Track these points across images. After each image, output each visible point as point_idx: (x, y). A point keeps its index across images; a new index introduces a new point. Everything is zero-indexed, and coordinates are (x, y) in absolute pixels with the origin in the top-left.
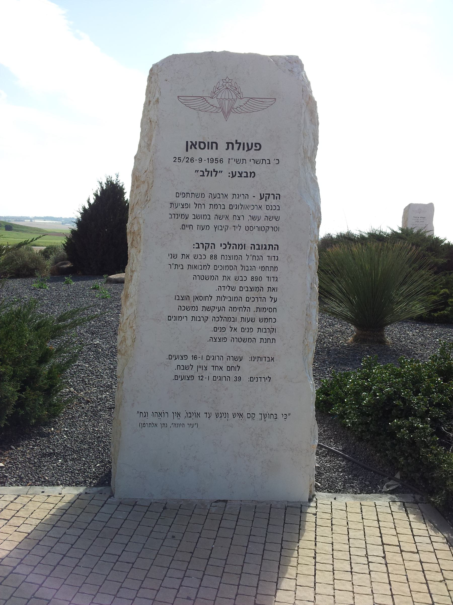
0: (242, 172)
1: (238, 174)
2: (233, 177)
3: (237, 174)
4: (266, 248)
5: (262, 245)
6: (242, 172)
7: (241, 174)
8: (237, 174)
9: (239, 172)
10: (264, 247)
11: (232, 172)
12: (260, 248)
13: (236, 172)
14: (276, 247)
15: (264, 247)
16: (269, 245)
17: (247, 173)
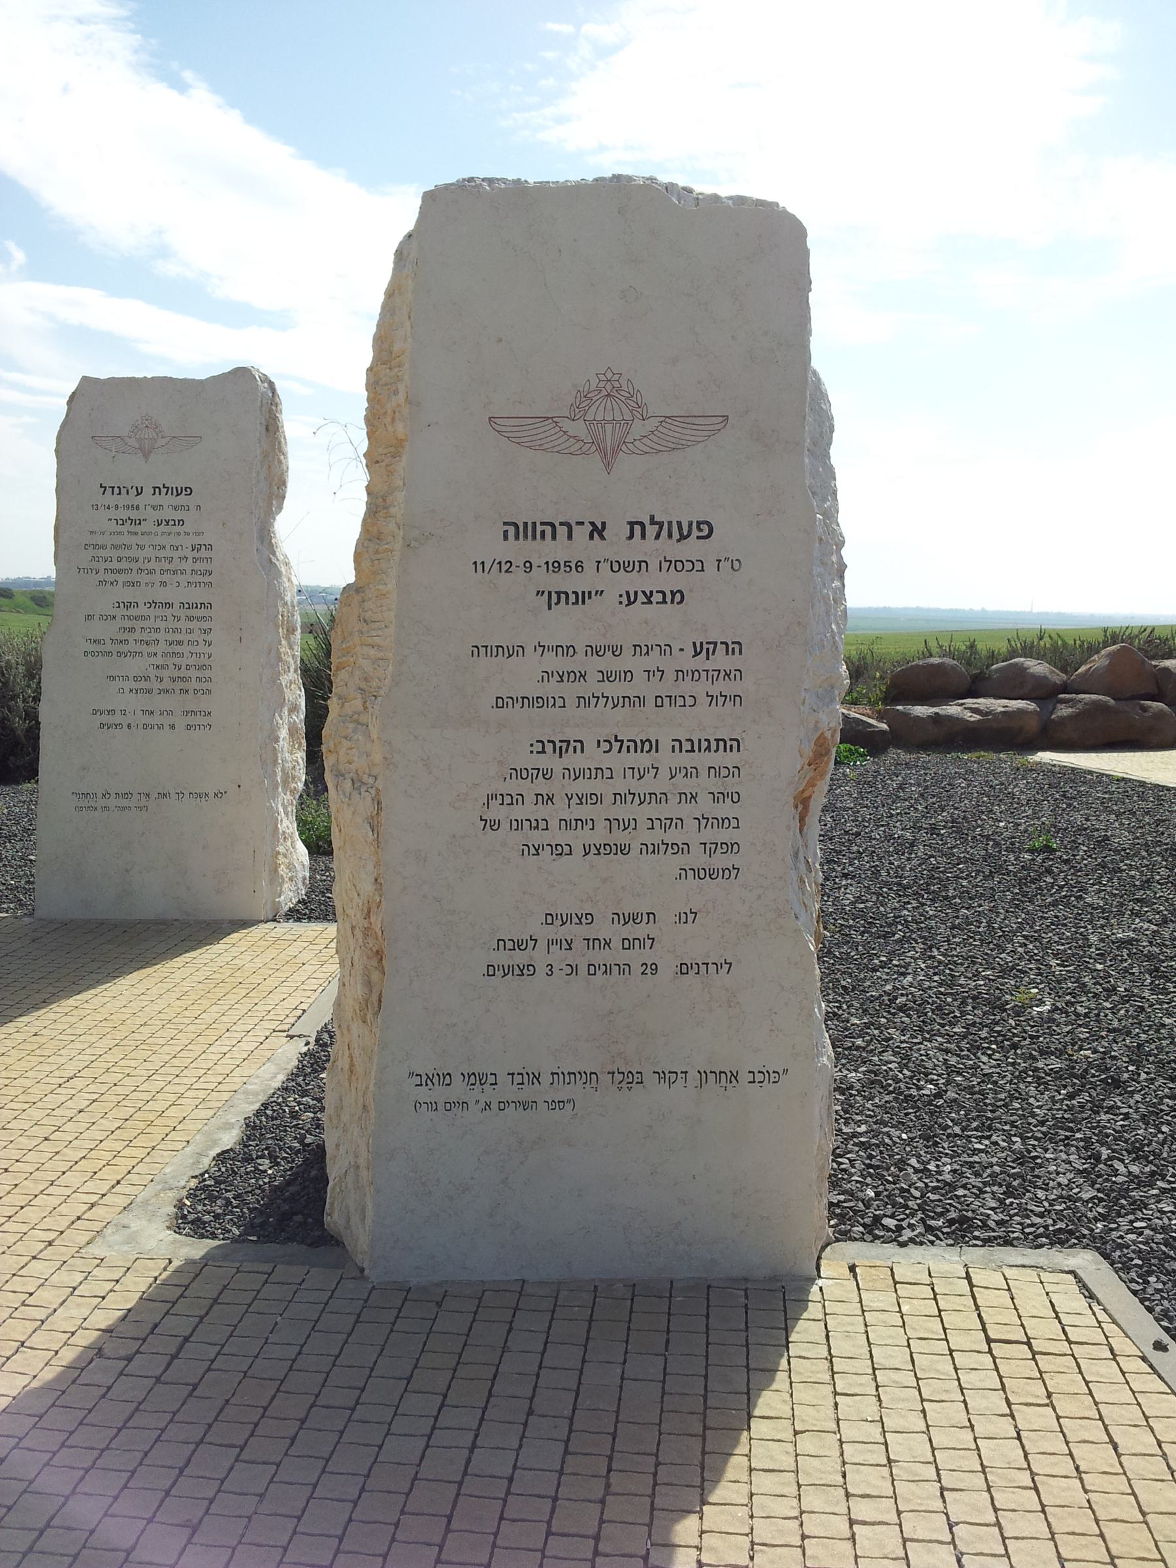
0: (651, 592)
4: (708, 748)
6: (651, 592)
8: (640, 594)
9: (644, 592)
10: (704, 745)
14: (735, 744)
15: (704, 745)
16: (717, 740)
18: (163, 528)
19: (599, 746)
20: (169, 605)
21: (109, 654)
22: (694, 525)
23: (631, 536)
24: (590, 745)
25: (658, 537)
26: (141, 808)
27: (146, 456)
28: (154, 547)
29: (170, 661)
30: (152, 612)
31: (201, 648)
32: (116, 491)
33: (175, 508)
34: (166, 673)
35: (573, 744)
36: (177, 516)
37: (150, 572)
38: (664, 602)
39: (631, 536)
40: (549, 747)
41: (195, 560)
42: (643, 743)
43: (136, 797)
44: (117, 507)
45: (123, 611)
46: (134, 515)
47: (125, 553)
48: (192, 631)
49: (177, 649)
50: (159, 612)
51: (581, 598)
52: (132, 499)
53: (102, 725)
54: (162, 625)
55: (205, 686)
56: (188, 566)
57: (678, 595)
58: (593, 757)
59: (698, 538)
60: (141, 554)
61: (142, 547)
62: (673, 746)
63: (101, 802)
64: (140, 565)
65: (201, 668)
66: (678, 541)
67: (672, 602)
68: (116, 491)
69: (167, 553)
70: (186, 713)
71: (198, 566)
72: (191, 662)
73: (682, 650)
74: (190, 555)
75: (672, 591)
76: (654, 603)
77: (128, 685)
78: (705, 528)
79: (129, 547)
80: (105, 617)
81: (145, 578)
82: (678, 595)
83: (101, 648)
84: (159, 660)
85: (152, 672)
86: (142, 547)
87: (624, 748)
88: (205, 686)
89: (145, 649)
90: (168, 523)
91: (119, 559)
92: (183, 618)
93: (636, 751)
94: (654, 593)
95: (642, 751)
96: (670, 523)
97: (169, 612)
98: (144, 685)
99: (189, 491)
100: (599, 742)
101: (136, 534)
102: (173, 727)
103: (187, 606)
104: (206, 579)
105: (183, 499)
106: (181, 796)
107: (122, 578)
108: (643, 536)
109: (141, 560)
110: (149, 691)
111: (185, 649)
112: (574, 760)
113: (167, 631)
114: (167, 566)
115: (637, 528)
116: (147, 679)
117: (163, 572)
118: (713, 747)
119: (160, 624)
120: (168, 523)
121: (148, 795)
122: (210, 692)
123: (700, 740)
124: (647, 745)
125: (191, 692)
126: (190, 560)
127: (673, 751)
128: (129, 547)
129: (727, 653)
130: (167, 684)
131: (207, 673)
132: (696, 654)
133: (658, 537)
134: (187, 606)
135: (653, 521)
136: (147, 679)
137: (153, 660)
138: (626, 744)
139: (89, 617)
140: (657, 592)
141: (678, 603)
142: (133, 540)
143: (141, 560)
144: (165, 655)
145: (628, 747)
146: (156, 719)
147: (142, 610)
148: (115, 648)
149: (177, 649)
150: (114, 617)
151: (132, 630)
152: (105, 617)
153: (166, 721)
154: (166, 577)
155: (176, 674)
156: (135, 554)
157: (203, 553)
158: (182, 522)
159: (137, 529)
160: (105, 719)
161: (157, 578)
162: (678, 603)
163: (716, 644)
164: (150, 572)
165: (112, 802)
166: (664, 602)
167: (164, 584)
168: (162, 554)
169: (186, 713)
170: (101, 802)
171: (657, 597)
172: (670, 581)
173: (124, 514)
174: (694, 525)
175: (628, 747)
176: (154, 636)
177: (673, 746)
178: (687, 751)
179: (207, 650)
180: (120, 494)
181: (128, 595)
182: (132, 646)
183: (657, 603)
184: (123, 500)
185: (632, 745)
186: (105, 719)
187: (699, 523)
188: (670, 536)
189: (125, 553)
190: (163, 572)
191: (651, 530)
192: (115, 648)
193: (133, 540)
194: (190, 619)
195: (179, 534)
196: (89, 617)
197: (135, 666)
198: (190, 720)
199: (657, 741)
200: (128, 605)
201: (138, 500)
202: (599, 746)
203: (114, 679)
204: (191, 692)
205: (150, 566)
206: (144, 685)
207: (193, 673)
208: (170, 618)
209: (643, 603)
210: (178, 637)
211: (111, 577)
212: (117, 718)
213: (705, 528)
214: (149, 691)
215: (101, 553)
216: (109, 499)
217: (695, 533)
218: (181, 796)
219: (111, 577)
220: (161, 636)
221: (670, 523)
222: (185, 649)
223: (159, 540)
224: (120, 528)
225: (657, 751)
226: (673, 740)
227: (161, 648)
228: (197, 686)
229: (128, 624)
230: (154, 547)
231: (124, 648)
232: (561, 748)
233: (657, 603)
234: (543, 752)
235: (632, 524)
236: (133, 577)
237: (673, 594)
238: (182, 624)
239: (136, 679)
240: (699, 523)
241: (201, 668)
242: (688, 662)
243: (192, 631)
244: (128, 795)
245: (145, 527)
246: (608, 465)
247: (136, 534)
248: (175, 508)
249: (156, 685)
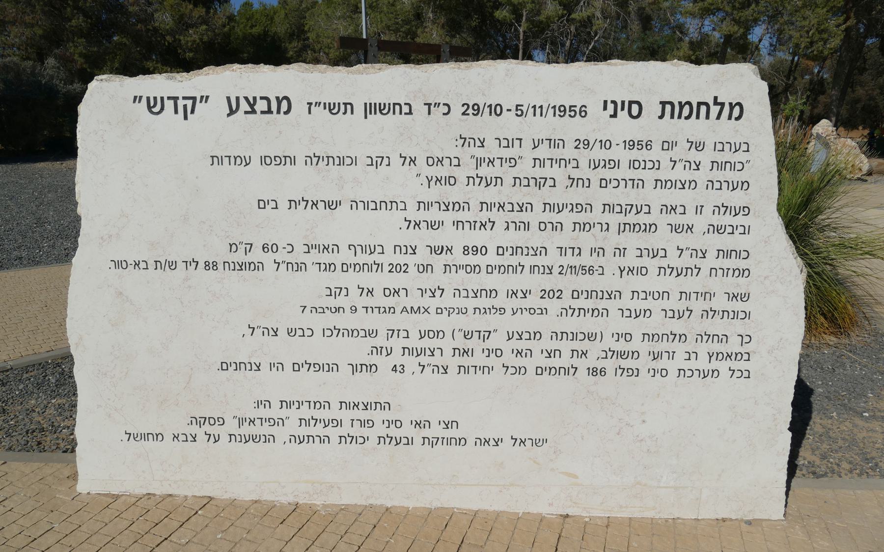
0: (255, 98)
1: (244, 106)
2: (232, 112)
6: (255, 98)
7: (252, 106)
8: (243, 103)
9: (246, 99)
13: (238, 99)
57: (284, 104)
67: (278, 112)
75: (277, 98)
76: (259, 112)
82: (284, 104)
94: (258, 99)
140: (262, 98)
141: (286, 113)
162: (286, 113)
166: (269, 111)
171: (261, 105)
183: (262, 112)
209: (246, 112)
233: (262, 112)
237: (279, 101)
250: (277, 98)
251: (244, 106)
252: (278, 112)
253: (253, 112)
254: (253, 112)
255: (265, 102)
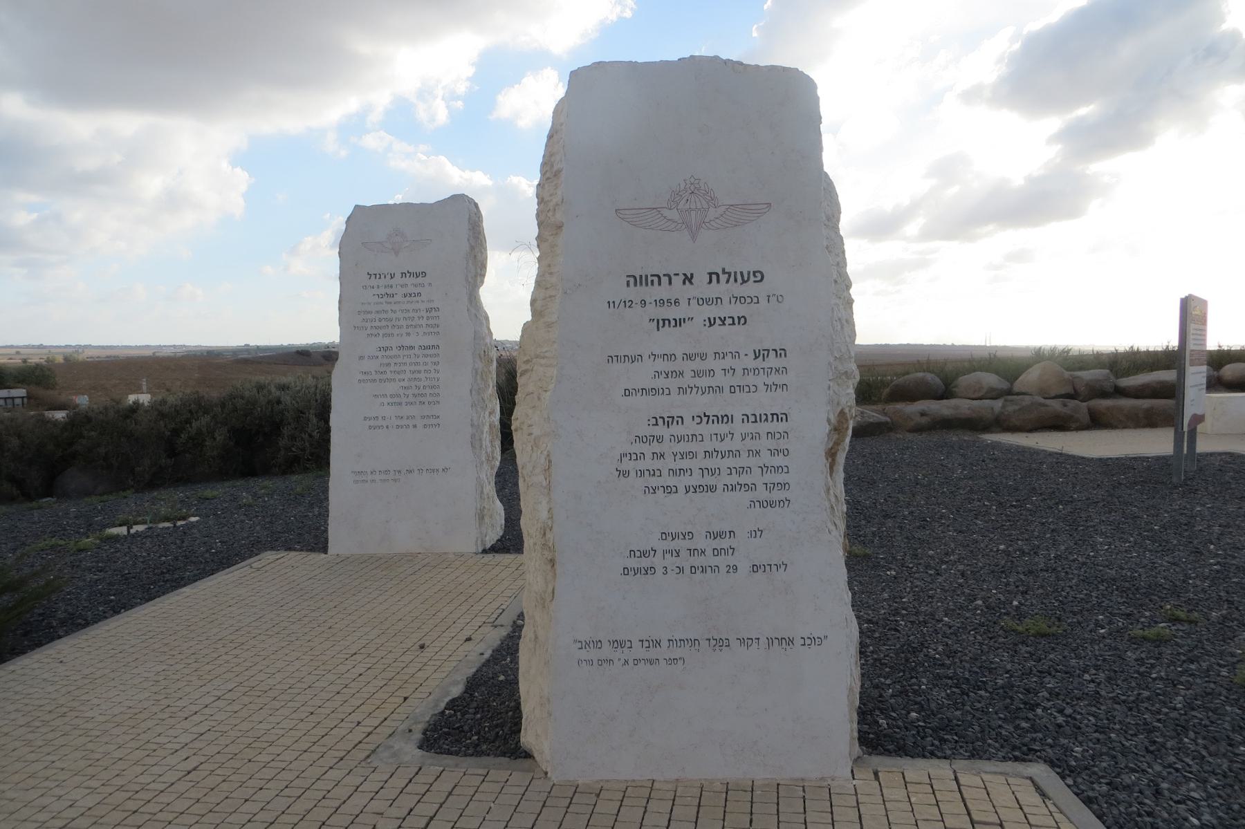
0: (725, 318)
1: (718, 321)
3: (718, 320)
5: (760, 415)
6: (725, 318)
8: (718, 320)
9: (720, 318)
10: (764, 417)
11: (709, 319)
12: (758, 419)
13: (715, 319)
14: (784, 417)
15: (764, 417)
16: (772, 414)
17: (733, 318)
18: (408, 298)
19: (693, 419)
20: (412, 348)
21: (374, 380)
22: (752, 273)
23: (710, 281)
24: (688, 420)
25: (728, 281)
26: (395, 480)
27: (397, 253)
28: (402, 311)
29: (413, 384)
30: (401, 353)
31: (433, 375)
32: (378, 276)
33: (416, 286)
34: (410, 392)
35: (676, 419)
36: (417, 291)
37: (400, 327)
38: (734, 324)
39: (710, 281)
40: (660, 421)
41: (428, 318)
42: (722, 417)
43: (392, 473)
44: (378, 287)
45: (383, 353)
46: (389, 291)
47: (383, 316)
48: (426, 364)
49: (417, 376)
50: (406, 352)
51: (679, 323)
52: (388, 281)
53: (370, 427)
54: (408, 360)
55: (435, 399)
56: (423, 322)
58: (690, 427)
59: (755, 282)
60: (394, 316)
61: (394, 312)
62: (743, 419)
63: (370, 477)
64: (394, 322)
65: (432, 387)
66: (741, 284)
67: (739, 323)
68: (378, 276)
69: (411, 314)
70: (423, 417)
71: (431, 322)
72: (426, 383)
73: (746, 355)
74: (425, 315)
75: (738, 317)
76: (727, 324)
77: (386, 401)
78: (758, 275)
79: (386, 312)
80: (371, 357)
81: (396, 331)
83: (370, 377)
84: (405, 384)
85: (401, 392)
86: (394, 312)
87: (710, 421)
88: (435, 399)
89: (398, 377)
90: (411, 295)
91: (380, 320)
92: (421, 356)
93: (718, 422)
95: (722, 422)
96: (735, 273)
97: (412, 352)
98: (396, 400)
99: (424, 274)
100: (693, 417)
101: (391, 303)
102: (415, 426)
103: (423, 348)
104: (436, 330)
105: (420, 280)
106: (421, 471)
107: (381, 332)
108: (718, 281)
109: (394, 319)
110: (400, 404)
111: (422, 376)
112: (676, 429)
113: (411, 364)
114: (410, 323)
115: (714, 277)
116: (399, 396)
117: (408, 327)
118: (770, 417)
119: (408, 360)
120: (411, 295)
121: (399, 472)
122: (438, 402)
123: (760, 415)
124: (725, 419)
125: (426, 403)
126: (425, 318)
127: (743, 422)
128: (386, 312)
129: (777, 356)
130: (411, 399)
131: (436, 391)
132: (756, 358)
133: (728, 281)
134: (423, 348)
135: (724, 272)
136: (399, 396)
137: (402, 384)
138: (711, 418)
139: (361, 358)
140: (729, 317)
142: (388, 307)
143: (394, 319)
144: (410, 380)
145: (713, 420)
146: (405, 422)
147: (395, 352)
148: (377, 377)
149: (417, 376)
150: (377, 357)
151: (388, 365)
152: (371, 357)
153: (411, 422)
154: (409, 330)
155: (416, 392)
156: (390, 315)
157: (434, 314)
158: (419, 294)
159: (391, 300)
160: (372, 423)
161: (404, 331)
163: (768, 350)
164: (400, 327)
165: (377, 477)
166: (734, 324)
167: (408, 334)
168: (406, 315)
169: (423, 417)
170: (370, 477)
171: (729, 321)
172: (737, 310)
173: (382, 291)
174: (752, 273)
175: (713, 420)
176: (403, 368)
177: (743, 419)
178: (752, 422)
179: (437, 375)
180: (380, 278)
181: (386, 342)
182: (389, 375)
183: (729, 324)
184: (382, 282)
185: (715, 418)
186: (372, 423)
187: (754, 273)
188: (736, 280)
189: (383, 316)
190: (408, 327)
191: (723, 278)
192: (377, 377)
193: (388, 307)
194: (426, 356)
195: (418, 302)
196: (361, 358)
197: (391, 388)
198: (426, 421)
199: (732, 416)
200: (386, 349)
201: (392, 282)
202: (693, 419)
203: (378, 396)
204: (426, 403)
205: (400, 323)
206: (396, 400)
207: (428, 391)
208: (413, 356)
209: (720, 325)
210: (417, 368)
211: (374, 331)
212: (380, 422)
213: (758, 275)
214: (400, 404)
215: (369, 316)
216: (374, 282)
217: (752, 278)
218: (421, 471)
219: (374, 331)
220: (407, 368)
221: (735, 273)
222: (422, 376)
223: (404, 307)
224: (381, 300)
225: (732, 422)
226: (743, 415)
227: (408, 375)
228: (431, 399)
229: (386, 361)
230: (402, 311)
231: (384, 377)
232: (668, 422)
233: (729, 324)
234: (657, 424)
235: (710, 274)
236: (389, 331)
237: (739, 318)
238: (421, 360)
239: (392, 396)
240: (754, 273)
241: (432, 387)
242: (750, 363)
243: (426, 364)
244: (387, 472)
245: (397, 298)
246: (694, 238)
247: (391, 303)
248: (416, 286)
249: (404, 400)
250: (738, 317)
251: (718, 321)
252: (739, 323)
253: (724, 324)
254: (724, 324)
255: (731, 320)
